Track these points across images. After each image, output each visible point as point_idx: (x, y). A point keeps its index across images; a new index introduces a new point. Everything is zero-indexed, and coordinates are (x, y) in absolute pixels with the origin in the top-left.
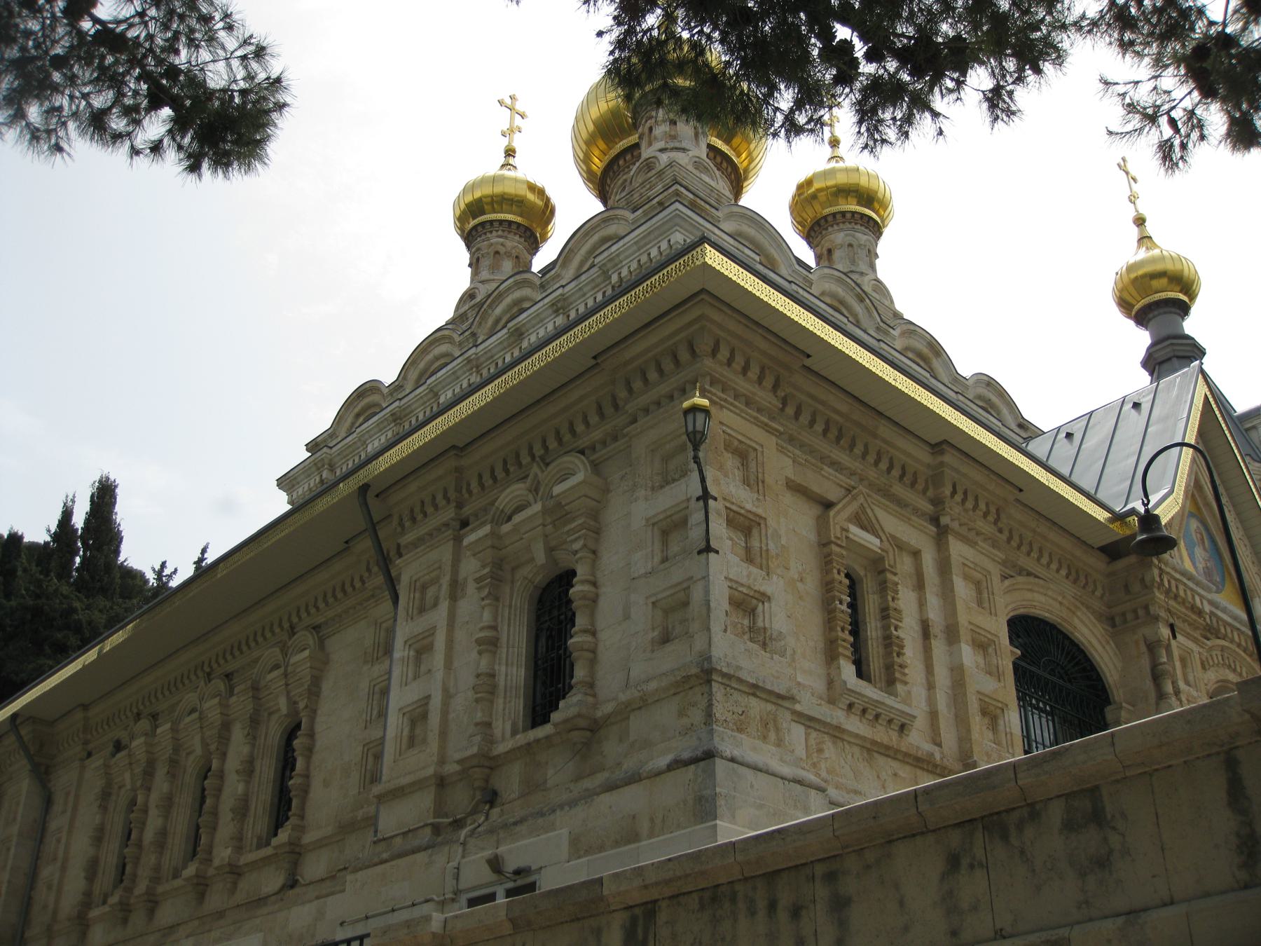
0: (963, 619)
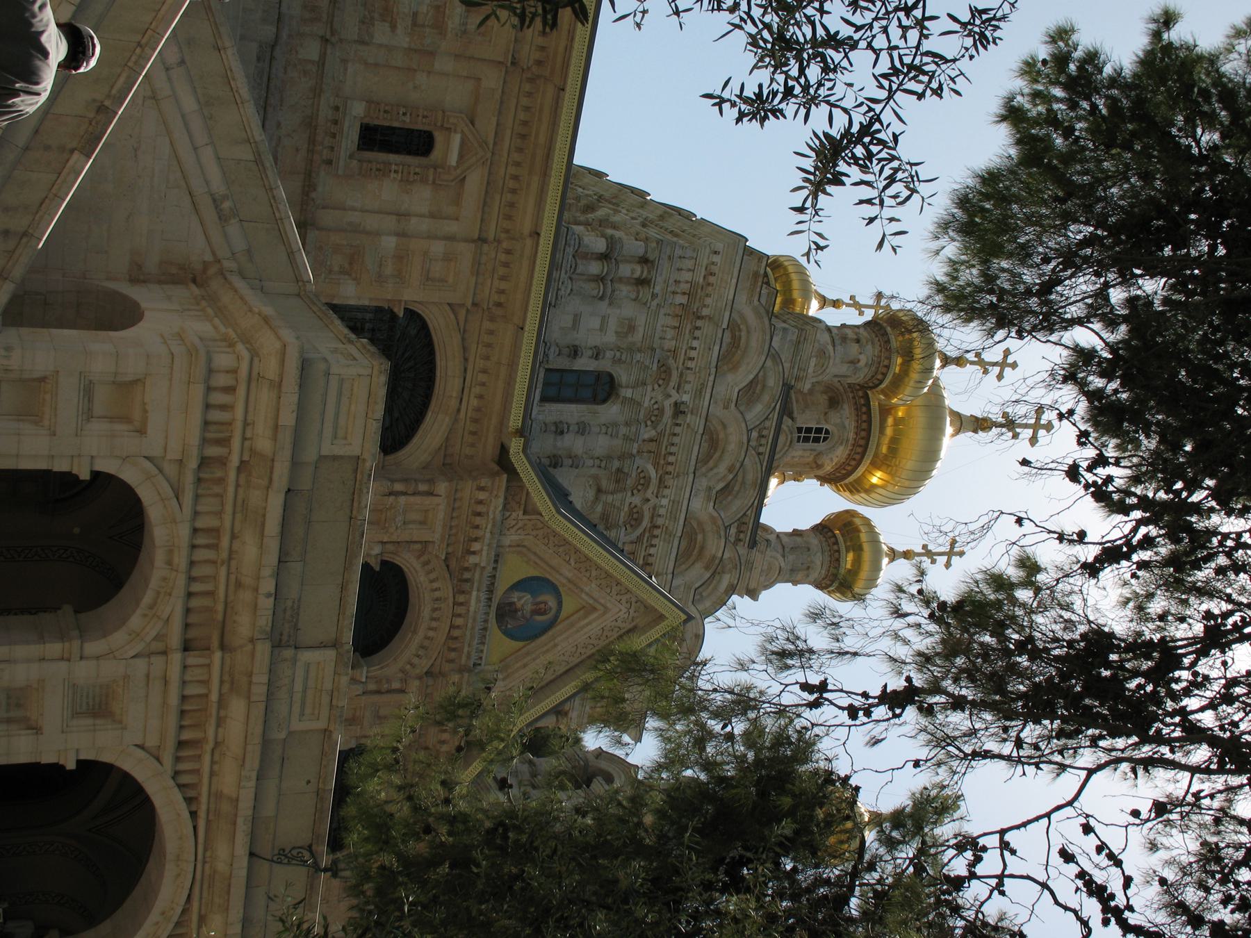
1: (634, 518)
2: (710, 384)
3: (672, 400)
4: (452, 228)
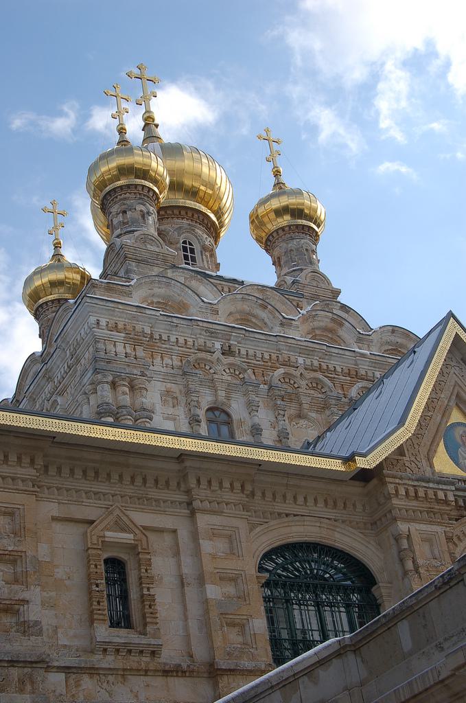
0: (208, 566)
1: (316, 385)
3: (222, 357)
4: (184, 535)
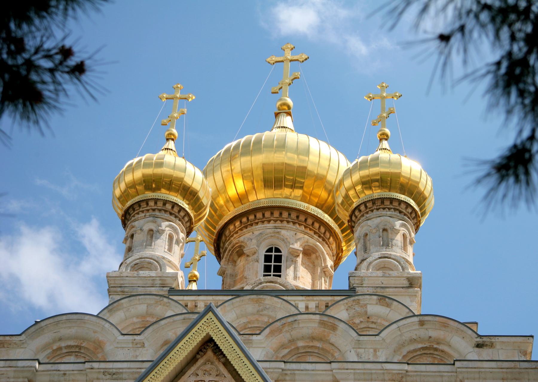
2: (103, 365)
